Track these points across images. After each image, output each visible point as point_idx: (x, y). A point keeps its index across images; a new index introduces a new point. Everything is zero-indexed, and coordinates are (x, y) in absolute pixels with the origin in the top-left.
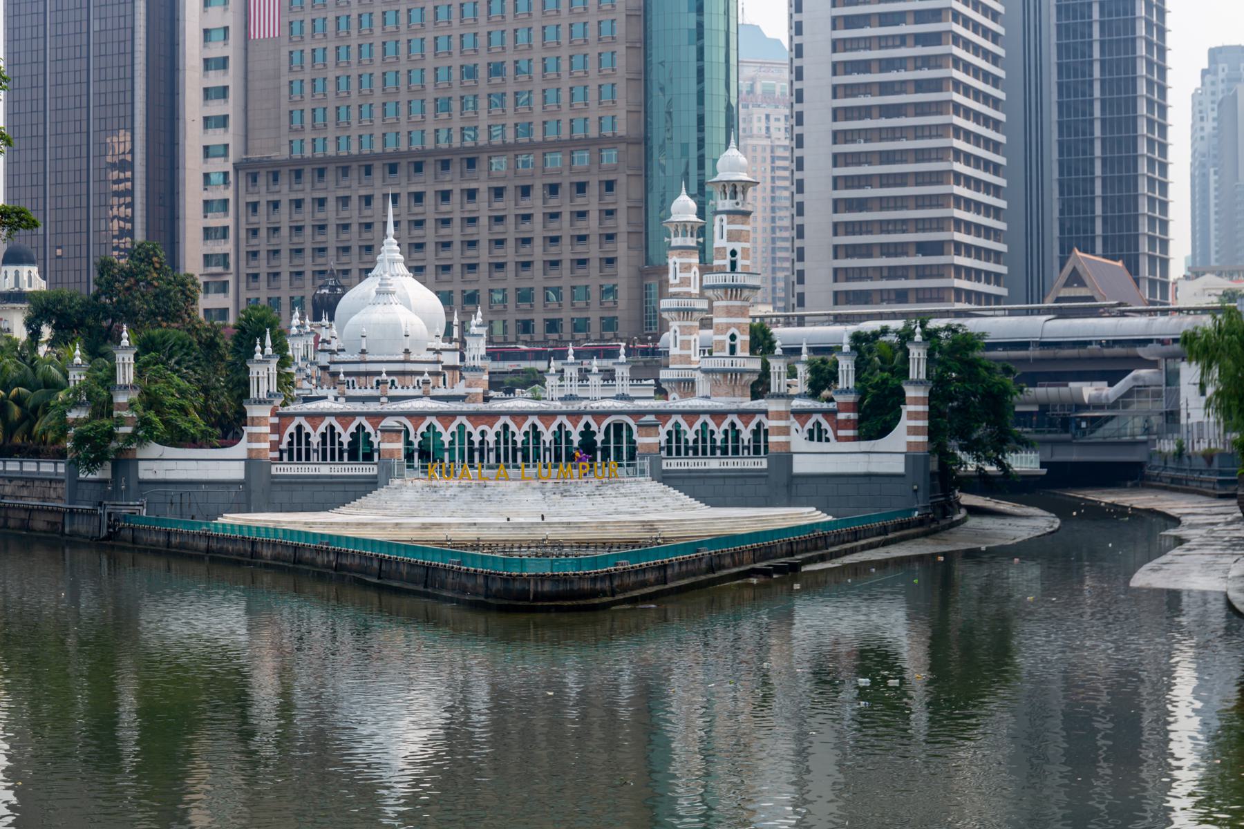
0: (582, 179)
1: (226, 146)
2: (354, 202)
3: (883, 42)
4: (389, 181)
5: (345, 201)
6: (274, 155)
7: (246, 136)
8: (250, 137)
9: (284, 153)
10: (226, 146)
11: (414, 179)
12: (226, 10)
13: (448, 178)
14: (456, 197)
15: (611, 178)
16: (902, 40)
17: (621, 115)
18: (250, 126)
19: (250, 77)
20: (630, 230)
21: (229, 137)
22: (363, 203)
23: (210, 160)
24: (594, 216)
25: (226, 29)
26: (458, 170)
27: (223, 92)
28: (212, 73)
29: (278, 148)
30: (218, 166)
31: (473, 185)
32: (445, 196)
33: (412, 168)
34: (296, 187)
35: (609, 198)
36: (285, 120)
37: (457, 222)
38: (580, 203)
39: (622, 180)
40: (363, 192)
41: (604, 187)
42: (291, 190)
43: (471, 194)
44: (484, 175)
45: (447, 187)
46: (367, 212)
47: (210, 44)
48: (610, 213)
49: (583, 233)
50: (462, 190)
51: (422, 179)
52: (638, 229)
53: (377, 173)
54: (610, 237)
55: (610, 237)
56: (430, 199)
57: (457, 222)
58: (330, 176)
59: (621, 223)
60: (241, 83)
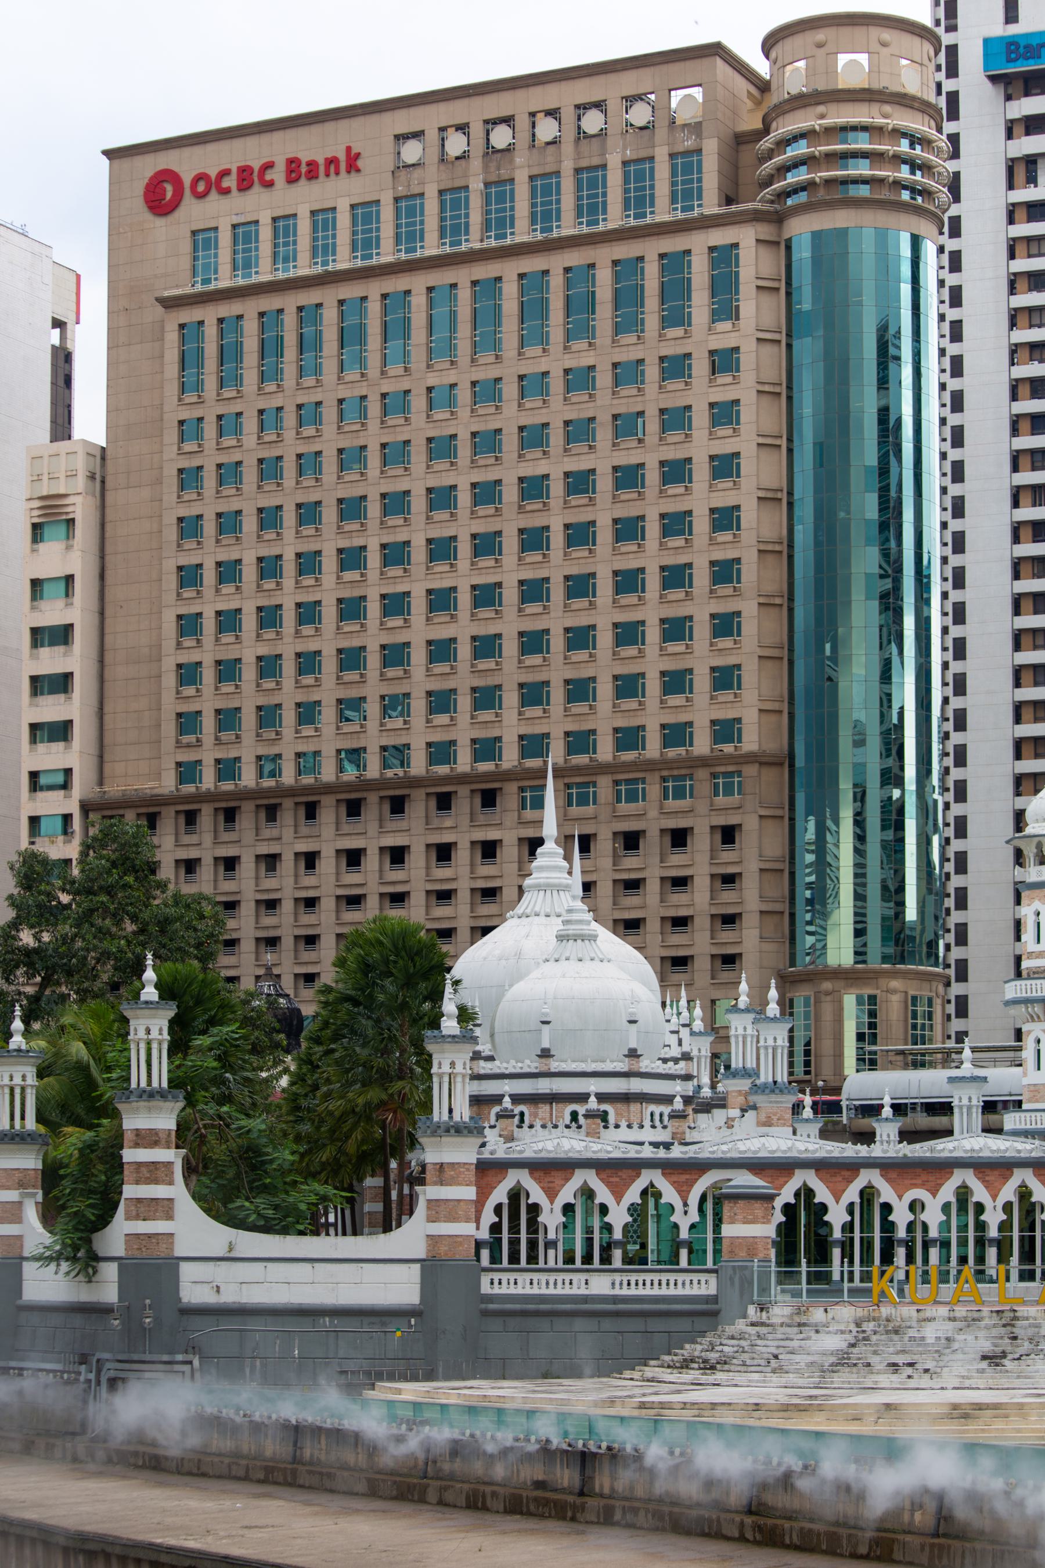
0: (681, 823)
1: (68, 772)
2: (287, 863)
4: (346, 828)
5: (271, 861)
6: (148, 787)
7: (101, 757)
8: (106, 757)
9: (168, 783)
10: (68, 772)
11: (390, 825)
12: (69, 548)
13: (448, 823)
14: (462, 855)
15: (732, 820)
17: (750, 718)
18: (107, 740)
19: (108, 658)
20: (765, 907)
21: (73, 755)
22: (302, 864)
23: (40, 795)
24: (702, 885)
25: (69, 579)
26: (467, 810)
27: (62, 683)
28: (45, 652)
29: (158, 776)
30: (52, 804)
31: (492, 835)
32: (444, 853)
33: (387, 807)
34: (186, 839)
35: (727, 855)
36: (169, 728)
37: (464, 896)
38: (677, 862)
39: (750, 823)
40: (303, 847)
41: (718, 837)
42: (178, 844)
43: (489, 850)
44: (510, 818)
45: (447, 838)
46: (309, 881)
47: (43, 605)
48: (729, 879)
49: (683, 912)
50: (473, 843)
51: (404, 825)
52: (778, 907)
53: (327, 815)
54: (730, 920)
55: (730, 920)
56: (417, 859)
57: (464, 896)
58: (246, 820)
59: (750, 897)
60: (93, 668)
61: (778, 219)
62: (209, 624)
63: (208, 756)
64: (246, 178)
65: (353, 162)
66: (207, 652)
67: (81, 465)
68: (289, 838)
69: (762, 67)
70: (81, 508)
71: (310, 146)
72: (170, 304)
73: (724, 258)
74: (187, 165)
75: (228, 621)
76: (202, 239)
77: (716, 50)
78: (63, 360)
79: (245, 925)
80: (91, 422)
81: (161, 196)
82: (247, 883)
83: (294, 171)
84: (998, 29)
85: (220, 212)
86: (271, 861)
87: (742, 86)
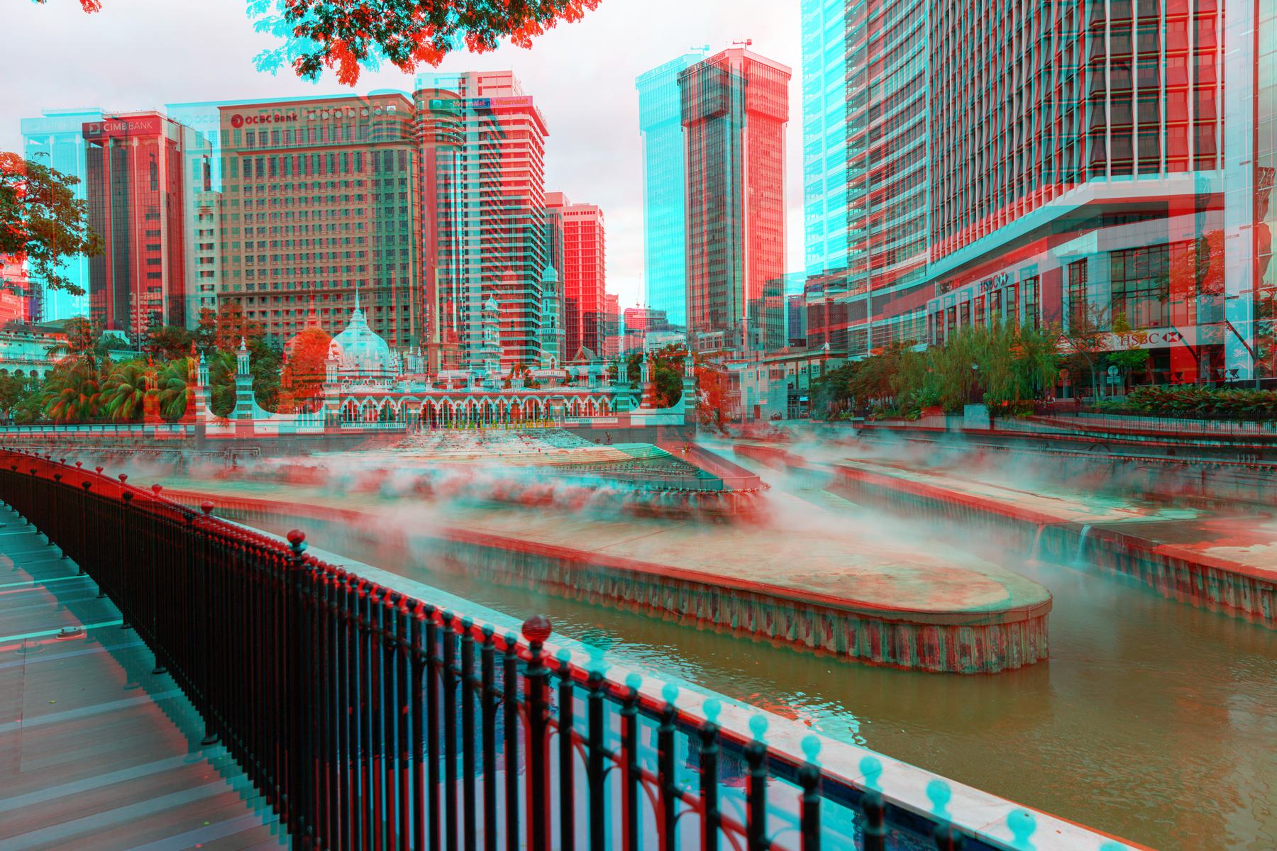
9: (244, 290)
16: (511, 258)
61: (417, 144)
62: (255, 245)
63: (256, 282)
64: (262, 120)
65: (295, 118)
66: (255, 253)
67: (214, 198)
68: (281, 306)
69: (412, 102)
70: (215, 211)
71: (283, 112)
72: (240, 153)
73: (402, 153)
74: (244, 114)
75: (262, 244)
76: (250, 135)
77: (399, 96)
78: (207, 168)
79: (269, 330)
80: (217, 184)
81: (237, 121)
82: (269, 318)
83: (277, 119)
84: (477, 97)
85: (256, 128)
86: (276, 312)
87: (407, 106)
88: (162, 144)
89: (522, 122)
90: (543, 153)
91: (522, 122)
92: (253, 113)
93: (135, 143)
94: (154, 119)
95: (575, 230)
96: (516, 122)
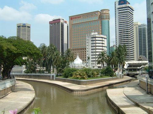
3: (124, 38)
16: (125, 38)
74: (73, 17)
77: (98, 11)
88: (61, 24)
89: (127, 9)
90: (133, 15)
91: (127, 9)
92: (74, 17)
93: (57, 24)
94: (59, 19)
95: (141, 30)
96: (126, 10)
